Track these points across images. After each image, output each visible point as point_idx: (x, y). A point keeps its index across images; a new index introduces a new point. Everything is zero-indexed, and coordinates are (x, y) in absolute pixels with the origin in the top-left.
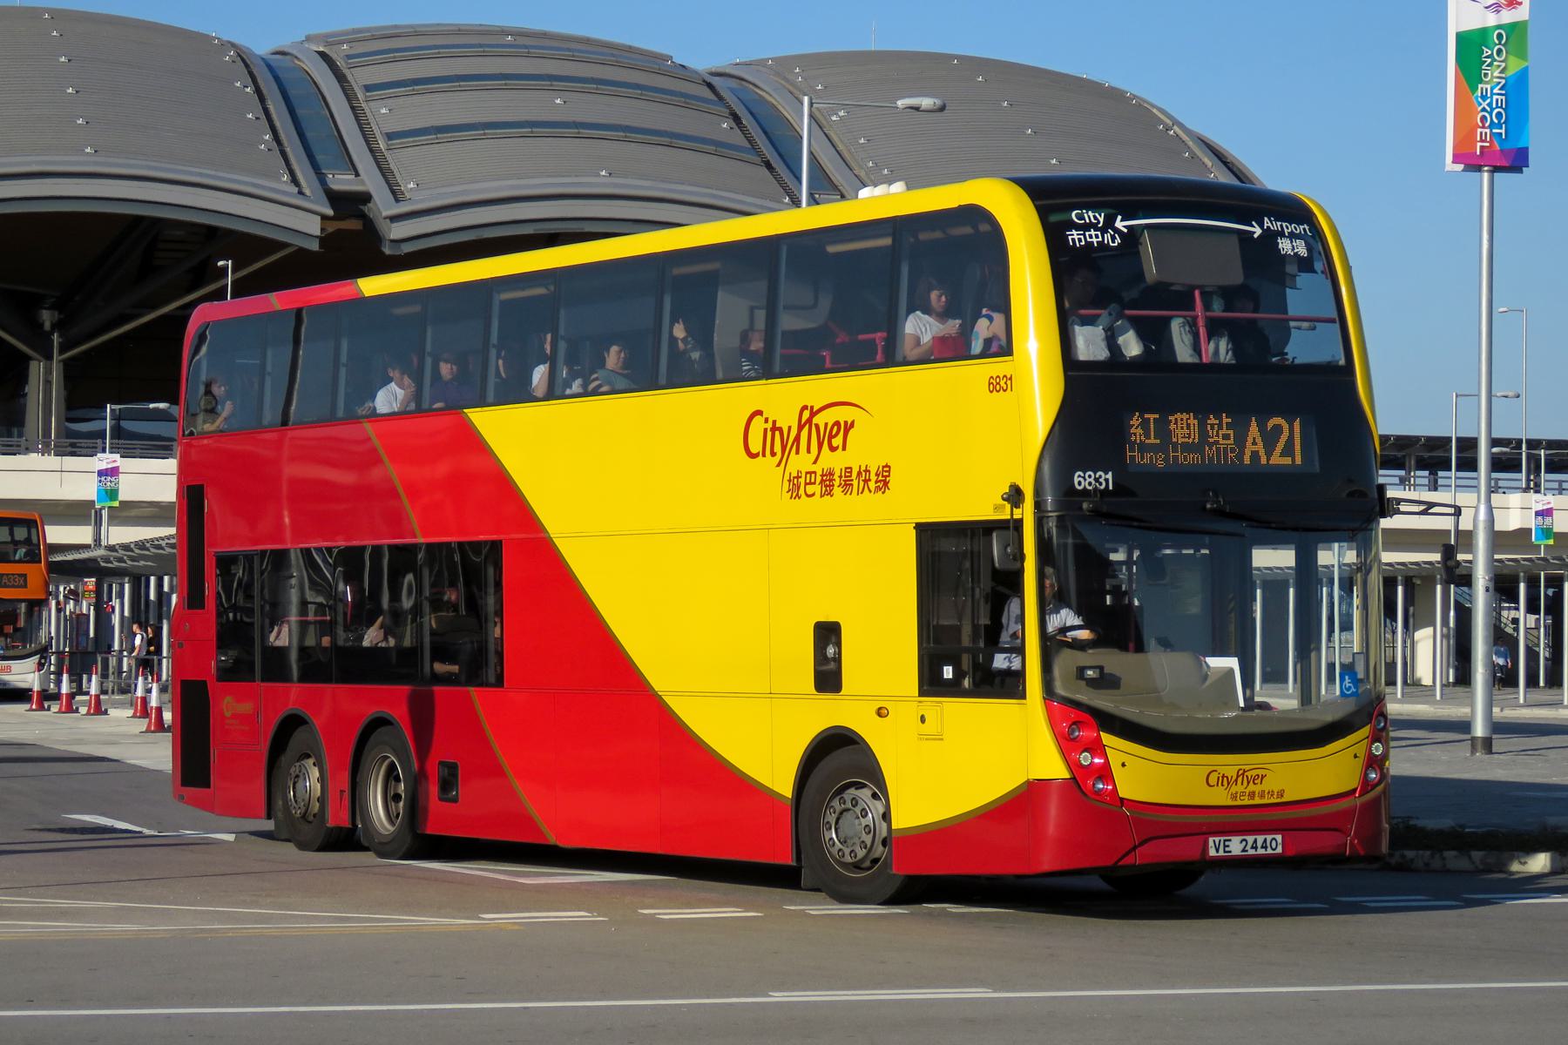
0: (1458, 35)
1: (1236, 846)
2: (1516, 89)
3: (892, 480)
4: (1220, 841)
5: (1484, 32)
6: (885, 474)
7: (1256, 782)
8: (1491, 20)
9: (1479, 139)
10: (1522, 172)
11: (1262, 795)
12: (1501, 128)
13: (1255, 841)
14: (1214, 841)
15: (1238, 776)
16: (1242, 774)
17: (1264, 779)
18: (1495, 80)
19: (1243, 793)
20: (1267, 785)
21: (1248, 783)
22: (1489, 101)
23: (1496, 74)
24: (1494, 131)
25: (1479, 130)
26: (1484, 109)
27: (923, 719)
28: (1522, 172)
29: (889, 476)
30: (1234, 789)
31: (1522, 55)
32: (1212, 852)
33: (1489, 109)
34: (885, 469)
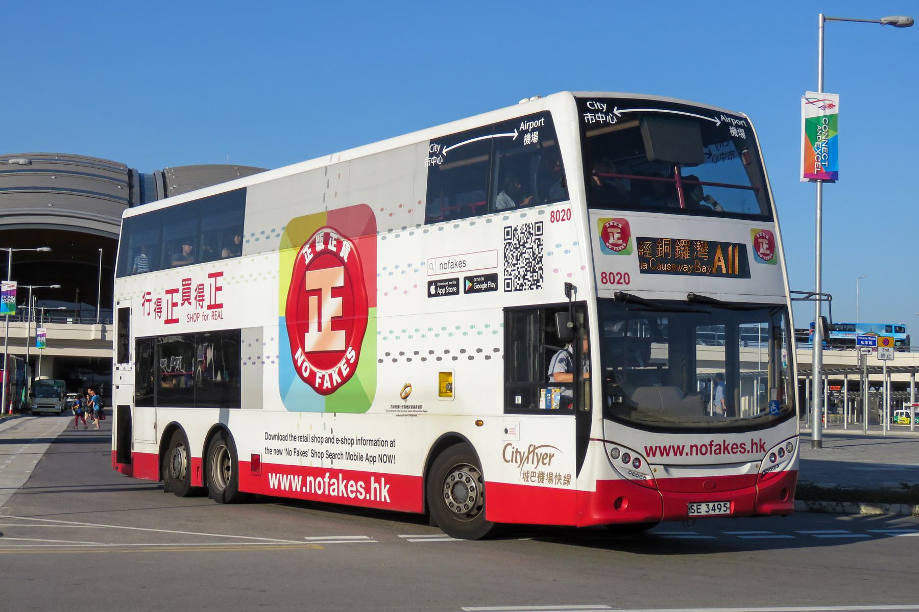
0: (806, 119)
2: (833, 145)
5: (818, 118)
8: (821, 113)
9: (815, 167)
10: (835, 182)
12: (826, 162)
18: (823, 140)
22: (820, 150)
23: (823, 138)
24: (823, 163)
25: (816, 163)
26: (818, 154)
28: (835, 182)
31: (835, 130)
33: (820, 153)
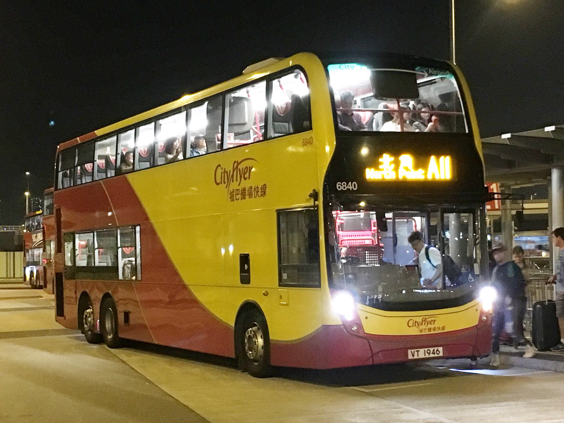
1: (422, 354)
3: (267, 191)
4: (414, 352)
6: (264, 188)
7: (431, 323)
11: (434, 329)
13: (434, 350)
14: (412, 352)
15: (423, 321)
16: (424, 320)
17: (435, 322)
19: (425, 329)
20: (436, 325)
21: (428, 324)
27: (281, 296)
29: (265, 189)
30: (421, 327)
32: (410, 357)
34: (265, 186)
